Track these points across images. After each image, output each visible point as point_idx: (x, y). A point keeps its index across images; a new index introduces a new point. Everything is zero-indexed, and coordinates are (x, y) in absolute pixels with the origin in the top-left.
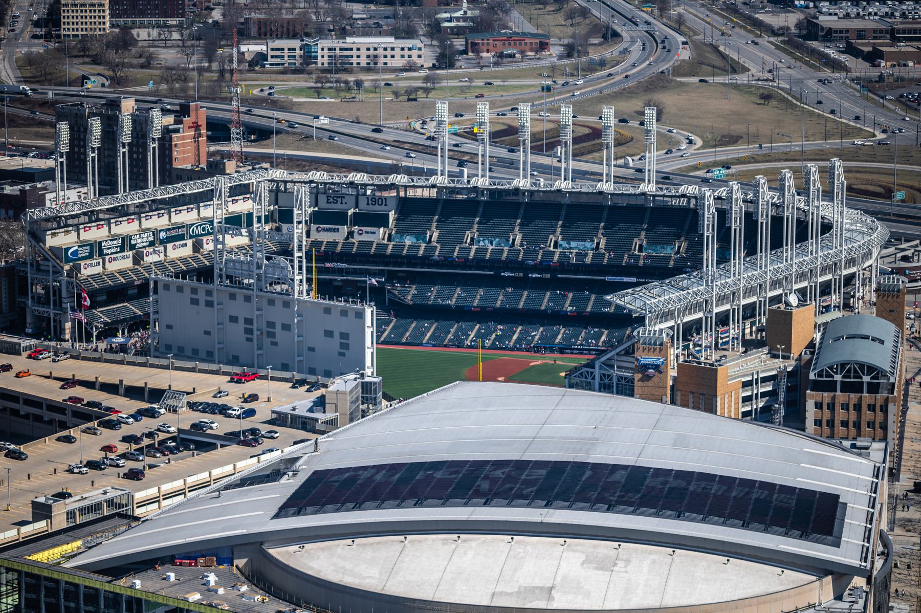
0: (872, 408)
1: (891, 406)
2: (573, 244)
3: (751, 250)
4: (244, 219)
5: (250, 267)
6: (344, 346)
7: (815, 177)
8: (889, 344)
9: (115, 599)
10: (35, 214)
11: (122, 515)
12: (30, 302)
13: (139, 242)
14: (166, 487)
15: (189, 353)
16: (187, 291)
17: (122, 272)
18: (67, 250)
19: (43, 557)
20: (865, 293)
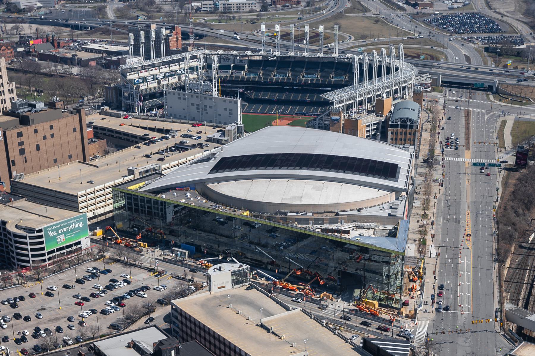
0: (410, 134)
1: (416, 133)
2: (309, 76)
3: (370, 77)
4: (195, 68)
5: (198, 86)
6: (231, 114)
7: (393, 50)
8: (417, 111)
9: (157, 202)
10: (123, 67)
11: (158, 173)
12: (123, 99)
13: (160, 76)
14: (172, 164)
15: (178, 116)
16: (177, 95)
17: (154, 88)
18: (135, 80)
19: (133, 187)
20: (409, 93)
